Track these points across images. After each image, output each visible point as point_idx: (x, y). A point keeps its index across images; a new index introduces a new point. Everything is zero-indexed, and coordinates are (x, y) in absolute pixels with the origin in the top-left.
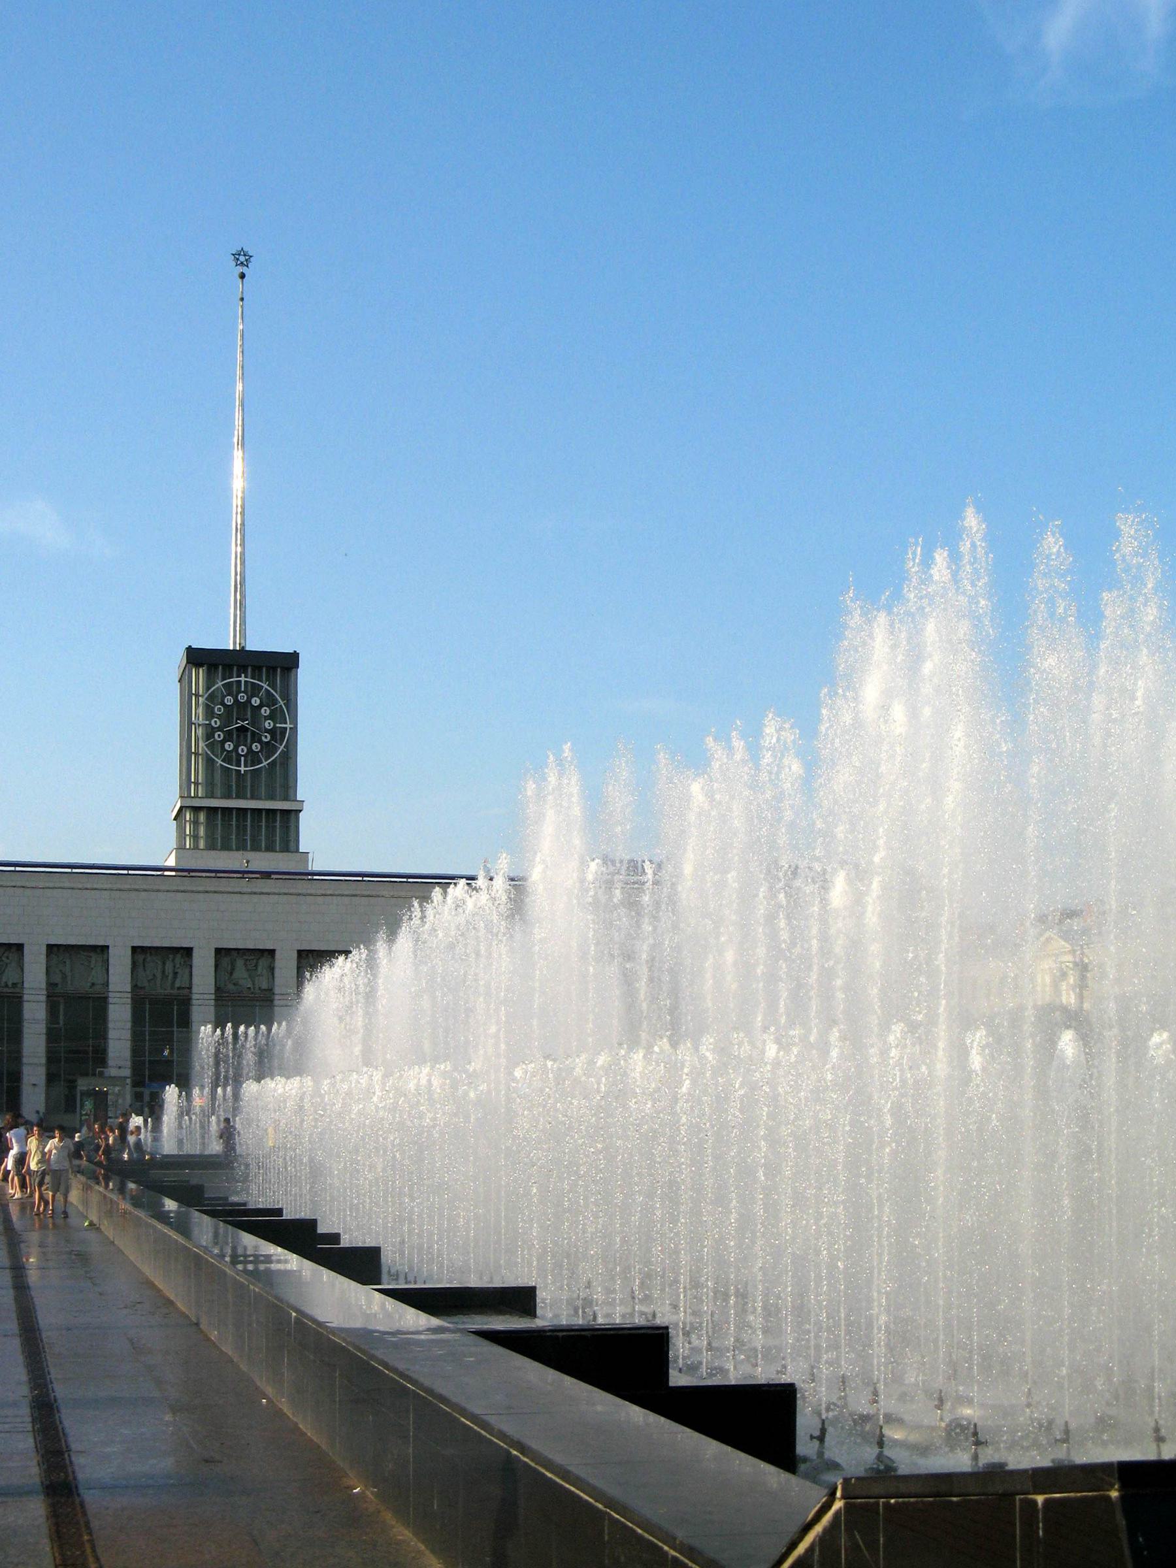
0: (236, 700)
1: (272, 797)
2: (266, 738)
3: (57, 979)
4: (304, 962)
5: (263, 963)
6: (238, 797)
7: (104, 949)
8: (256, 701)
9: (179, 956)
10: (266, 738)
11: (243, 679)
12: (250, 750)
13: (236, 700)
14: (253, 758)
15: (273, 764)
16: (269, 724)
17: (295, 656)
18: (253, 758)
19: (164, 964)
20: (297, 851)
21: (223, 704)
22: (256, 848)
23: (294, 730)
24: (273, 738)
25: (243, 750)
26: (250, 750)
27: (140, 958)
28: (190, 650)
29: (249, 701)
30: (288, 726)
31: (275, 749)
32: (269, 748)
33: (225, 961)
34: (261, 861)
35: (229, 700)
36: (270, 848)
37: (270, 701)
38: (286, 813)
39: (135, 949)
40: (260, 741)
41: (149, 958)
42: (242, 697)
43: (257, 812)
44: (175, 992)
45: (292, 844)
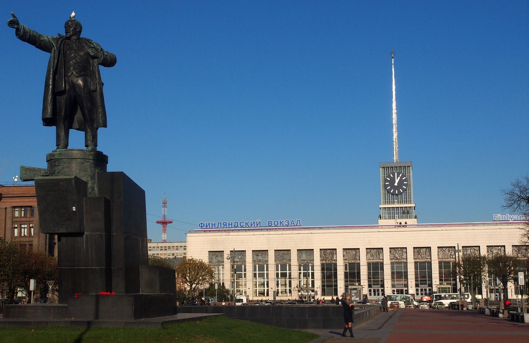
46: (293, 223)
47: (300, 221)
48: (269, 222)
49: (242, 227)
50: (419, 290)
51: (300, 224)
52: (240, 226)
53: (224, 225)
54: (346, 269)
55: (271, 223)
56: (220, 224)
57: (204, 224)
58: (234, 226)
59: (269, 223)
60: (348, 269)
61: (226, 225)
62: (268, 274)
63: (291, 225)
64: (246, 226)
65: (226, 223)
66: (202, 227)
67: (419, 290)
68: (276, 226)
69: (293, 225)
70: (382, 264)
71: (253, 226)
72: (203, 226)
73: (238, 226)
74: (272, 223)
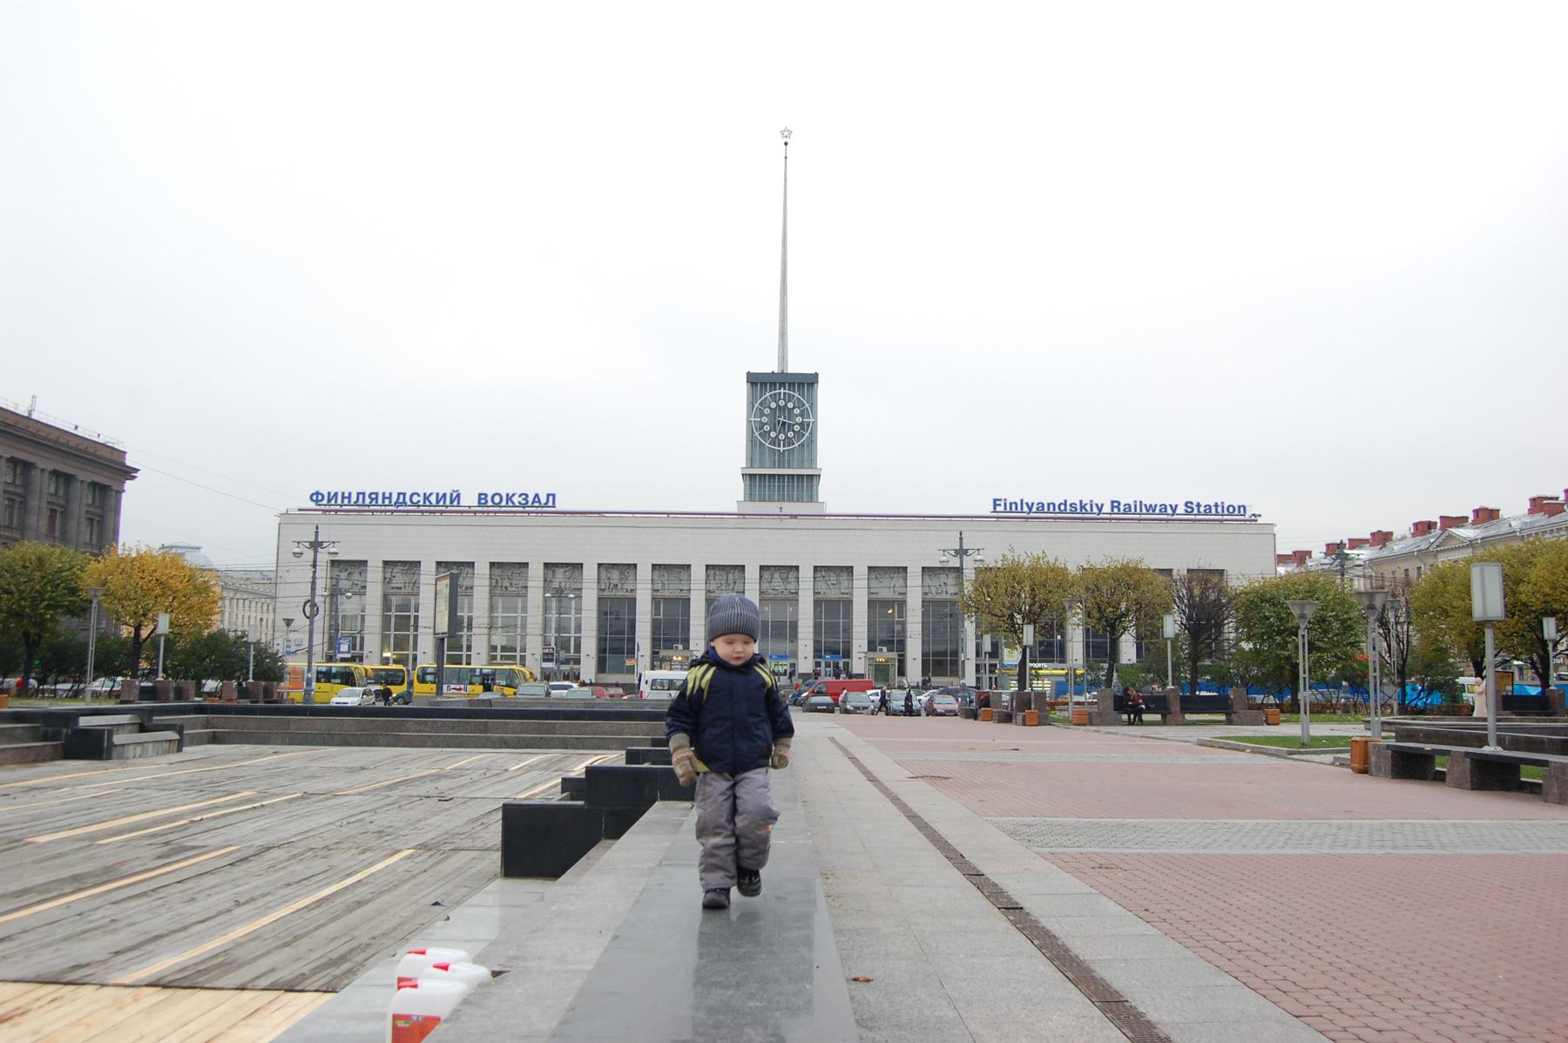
0: (778, 405)
2: (797, 428)
3: (659, 586)
4: (818, 574)
5: (792, 574)
6: (779, 467)
7: (689, 566)
8: (790, 405)
9: (737, 571)
10: (797, 428)
11: (782, 391)
12: (787, 437)
13: (778, 405)
14: (789, 441)
15: (803, 444)
16: (799, 420)
17: (817, 374)
19: (727, 576)
20: (817, 502)
21: (770, 408)
22: (791, 500)
23: (815, 423)
25: (782, 436)
26: (787, 437)
27: (711, 572)
28: (748, 373)
29: (786, 405)
30: (811, 420)
31: (804, 435)
32: (799, 435)
33: (766, 575)
34: (790, 507)
35: (773, 405)
36: (800, 500)
38: (812, 476)
39: (708, 567)
40: (793, 431)
41: (717, 573)
42: (782, 403)
45: (815, 499)
46: (537, 500)
47: (554, 495)
48: (480, 495)
49: (417, 504)
50: (823, 665)
51: (554, 503)
54: (657, 613)
55: (484, 499)
56: (361, 496)
57: (321, 494)
58: (397, 502)
59: (480, 499)
60: (662, 613)
61: (377, 499)
62: (472, 619)
63: (533, 503)
64: (424, 503)
65: (377, 494)
66: (317, 501)
67: (823, 665)
68: (496, 505)
71: (441, 503)
72: (320, 497)
73: (404, 503)
74: (489, 499)
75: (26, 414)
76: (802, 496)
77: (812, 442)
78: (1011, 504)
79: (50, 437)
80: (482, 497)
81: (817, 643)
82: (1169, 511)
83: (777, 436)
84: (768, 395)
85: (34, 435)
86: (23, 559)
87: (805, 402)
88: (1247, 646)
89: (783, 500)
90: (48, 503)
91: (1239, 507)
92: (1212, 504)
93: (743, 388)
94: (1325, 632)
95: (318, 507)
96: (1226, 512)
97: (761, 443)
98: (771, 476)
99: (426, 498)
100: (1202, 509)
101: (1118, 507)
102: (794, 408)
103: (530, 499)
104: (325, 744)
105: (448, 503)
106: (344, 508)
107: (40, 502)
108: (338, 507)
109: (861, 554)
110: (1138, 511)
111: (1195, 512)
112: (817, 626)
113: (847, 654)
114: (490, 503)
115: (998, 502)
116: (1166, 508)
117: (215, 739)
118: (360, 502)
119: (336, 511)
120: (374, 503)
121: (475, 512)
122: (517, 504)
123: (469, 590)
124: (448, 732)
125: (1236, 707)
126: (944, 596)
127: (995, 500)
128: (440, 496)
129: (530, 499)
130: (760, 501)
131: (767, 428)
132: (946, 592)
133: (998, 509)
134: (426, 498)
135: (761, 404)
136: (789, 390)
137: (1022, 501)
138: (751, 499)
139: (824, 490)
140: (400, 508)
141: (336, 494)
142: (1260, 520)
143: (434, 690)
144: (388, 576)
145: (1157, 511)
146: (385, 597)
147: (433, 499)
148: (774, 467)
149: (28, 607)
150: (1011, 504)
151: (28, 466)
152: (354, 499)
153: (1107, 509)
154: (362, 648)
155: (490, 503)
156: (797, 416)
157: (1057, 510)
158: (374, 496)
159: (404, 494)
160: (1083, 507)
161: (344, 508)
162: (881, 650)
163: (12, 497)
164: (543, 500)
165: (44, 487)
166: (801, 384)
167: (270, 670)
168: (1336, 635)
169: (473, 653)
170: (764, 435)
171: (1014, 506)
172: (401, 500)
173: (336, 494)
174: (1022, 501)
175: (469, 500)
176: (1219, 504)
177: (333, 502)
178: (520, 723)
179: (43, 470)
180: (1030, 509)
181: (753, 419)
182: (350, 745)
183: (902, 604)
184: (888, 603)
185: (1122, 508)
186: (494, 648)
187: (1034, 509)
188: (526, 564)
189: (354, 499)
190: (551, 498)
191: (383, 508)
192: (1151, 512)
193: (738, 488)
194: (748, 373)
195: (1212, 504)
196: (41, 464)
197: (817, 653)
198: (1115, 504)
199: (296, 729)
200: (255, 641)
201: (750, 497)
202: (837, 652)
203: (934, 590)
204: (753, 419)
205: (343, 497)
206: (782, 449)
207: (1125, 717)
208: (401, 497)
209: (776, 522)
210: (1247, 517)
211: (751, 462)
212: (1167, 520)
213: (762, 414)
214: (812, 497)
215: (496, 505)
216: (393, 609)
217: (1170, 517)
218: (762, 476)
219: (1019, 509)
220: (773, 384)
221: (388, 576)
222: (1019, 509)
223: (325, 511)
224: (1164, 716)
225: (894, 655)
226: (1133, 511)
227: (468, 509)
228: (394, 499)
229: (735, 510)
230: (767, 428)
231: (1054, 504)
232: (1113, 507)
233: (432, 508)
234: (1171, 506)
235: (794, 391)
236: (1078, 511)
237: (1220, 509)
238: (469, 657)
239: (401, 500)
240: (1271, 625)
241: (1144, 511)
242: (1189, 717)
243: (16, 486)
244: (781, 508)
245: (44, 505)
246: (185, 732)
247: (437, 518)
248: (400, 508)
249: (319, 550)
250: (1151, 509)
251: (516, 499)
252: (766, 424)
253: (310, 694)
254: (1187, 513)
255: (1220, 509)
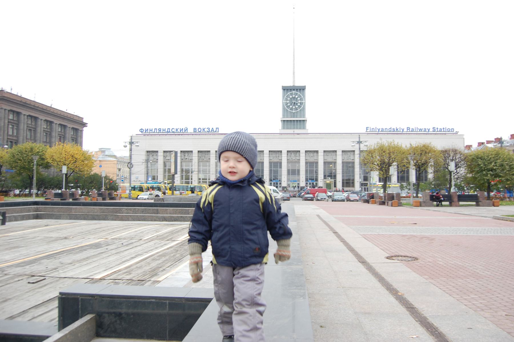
1: (301, 118)
2: (299, 104)
5: (298, 153)
6: (293, 118)
8: (297, 97)
10: (299, 104)
12: (296, 108)
14: (296, 109)
15: (301, 110)
16: (300, 101)
17: (305, 86)
18: (296, 109)
22: (297, 128)
23: (305, 102)
24: (301, 104)
25: (294, 107)
26: (296, 108)
27: (271, 153)
28: (282, 86)
29: (295, 97)
30: (304, 101)
31: (301, 107)
32: (300, 107)
33: (289, 153)
36: (300, 128)
37: (300, 96)
38: (304, 121)
41: (273, 153)
42: (294, 96)
43: (300, 121)
44: (279, 161)
45: (305, 128)
47: (218, 128)
48: (194, 128)
49: (174, 132)
50: (308, 183)
52: (171, 132)
53: (159, 131)
56: (156, 130)
58: (167, 132)
59: (194, 130)
61: (161, 130)
65: (161, 129)
66: (142, 132)
67: (308, 183)
68: (200, 132)
69: (213, 131)
70: (281, 163)
72: (143, 130)
73: (170, 132)
74: (197, 130)
75: (50, 106)
76: (301, 127)
77: (304, 109)
78: (372, 129)
79: (58, 113)
80: (195, 129)
81: (306, 176)
82: (427, 130)
83: (292, 107)
84: (289, 93)
85: (52, 112)
86: (26, 148)
87: (301, 95)
88: (470, 175)
89: (295, 129)
90: (58, 134)
91: (452, 129)
92: (442, 128)
93: (281, 91)
94: (503, 170)
95: (142, 134)
96: (447, 131)
97: (287, 110)
98: (291, 121)
99: (177, 130)
100: (439, 130)
101: (409, 129)
102: (298, 97)
103: (211, 130)
104: (85, 219)
105: (184, 131)
106: (150, 134)
107: (56, 134)
108: (148, 134)
109: (321, 146)
110: (416, 131)
111: (436, 131)
112: (306, 171)
113: (317, 180)
114: (197, 131)
115: (368, 128)
116: (426, 129)
117: (37, 217)
118: (155, 132)
119: (148, 135)
120: (160, 132)
121: (193, 134)
122: (206, 131)
123: (191, 160)
124: (141, 214)
125: (480, 199)
126: (349, 160)
127: (367, 128)
128: (181, 129)
129: (211, 130)
130: (287, 129)
131: (289, 105)
132: (350, 159)
133: (368, 130)
134: (177, 130)
135: (287, 96)
136: (296, 91)
137: (376, 128)
138: (284, 129)
139: (308, 125)
140: (168, 133)
141: (148, 129)
142: (459, 134)
143: (171, 193)
144: (165, 155)
145: (423, 131)
146: (164, 162)
147: (179, 130)
148: (291, 118)
149: (27, 165)
150: (372, 129)
151: (51, 122)
152: (153, 131)
153: (405, 130)
154: (157, 179)
155: (197, 131)
156: (299, 100)
157: (388, 131)
158: (160, 130)
159: (169, 129)
160: (397, 130)
161: (150, 134)
162: (328, 178)
163: (46, 132)
164: (215, 130)
165: (42, 126)
166: (300, 89)
167: (113, 187)
168: (508, 171)
169: (193, 181)
170: (288, 107)
171: (373, 129)
172: (169, 131)
173: (148, 129)
174: (376, 128)
175: (191, 130)
176: (445, 128)
177: (147, 132)
178: (173, 209)
179: (56, 124)
180: (379, 130)
181: (284, 102)
182: (95, 220)
183: (335, 163)
184: (330, 163)
185: (411, 130)
186: (200, 179)
187: (380, 130)
188: (209, 151)
189: (153, 131)
190: (217, 129)
191: (163, 133)
192: (421, 131)
193: (280, 124)
194: (282, 86)
195: (442, 128)
196: (55, 122)
197: (307, 180)
198: (408, 128)
199: (75, 212)
200: (105, 176)
201: (284, 128)
202: (313, 180)
203: (346, 159)
204: (284, 102)
205: (150, 130)
206: (294, 111)
207: (435, 203)
208: (169, 130)
209: (292, 136)
210: (454, 132)
211: (284, 116)
212: (426, 134)
213: (287, 100)
214: (304, 128)
215: (200, 132)
216: (167, 166)
217: (427, 133)
218: (288, 121)
219: (375, 131)
220: (291, 90)
221: (165, 155)
222: (375, 131)
223: (144, 135)
224: (450, 203)
225: (333, 180)
226: (414, 131)
227: (190, 133)
228: (166, 131)
229: (279, 132)
230: (289, 105)
231: (387, 129)
232: (407, 129)
233: (179, 133)
234: (428, 129)
235: (298, 92)
236: (396, 131)
237: (445, 130)
238: (192, 182)
239: (169, 131)
240: (482, 167)
241: (418, 131)
242: (461, 203)
243: (48, 129)
244: (294, 131)
245: (57, 135)
246: (7, 215)
247: (180, 137)
248: (168, 133)
249: (133, 145)
250: (421, 130)
251: (206, 130)
252: (289, 103)
253: (130, 195)
254: (433, 131)
255: (445, 130)
